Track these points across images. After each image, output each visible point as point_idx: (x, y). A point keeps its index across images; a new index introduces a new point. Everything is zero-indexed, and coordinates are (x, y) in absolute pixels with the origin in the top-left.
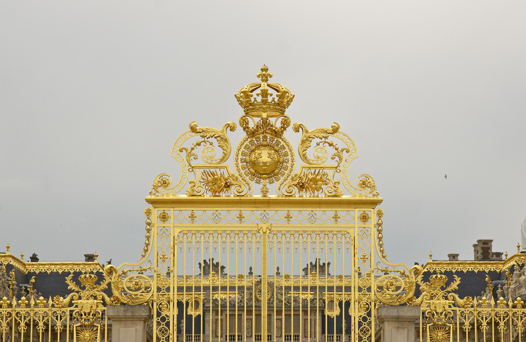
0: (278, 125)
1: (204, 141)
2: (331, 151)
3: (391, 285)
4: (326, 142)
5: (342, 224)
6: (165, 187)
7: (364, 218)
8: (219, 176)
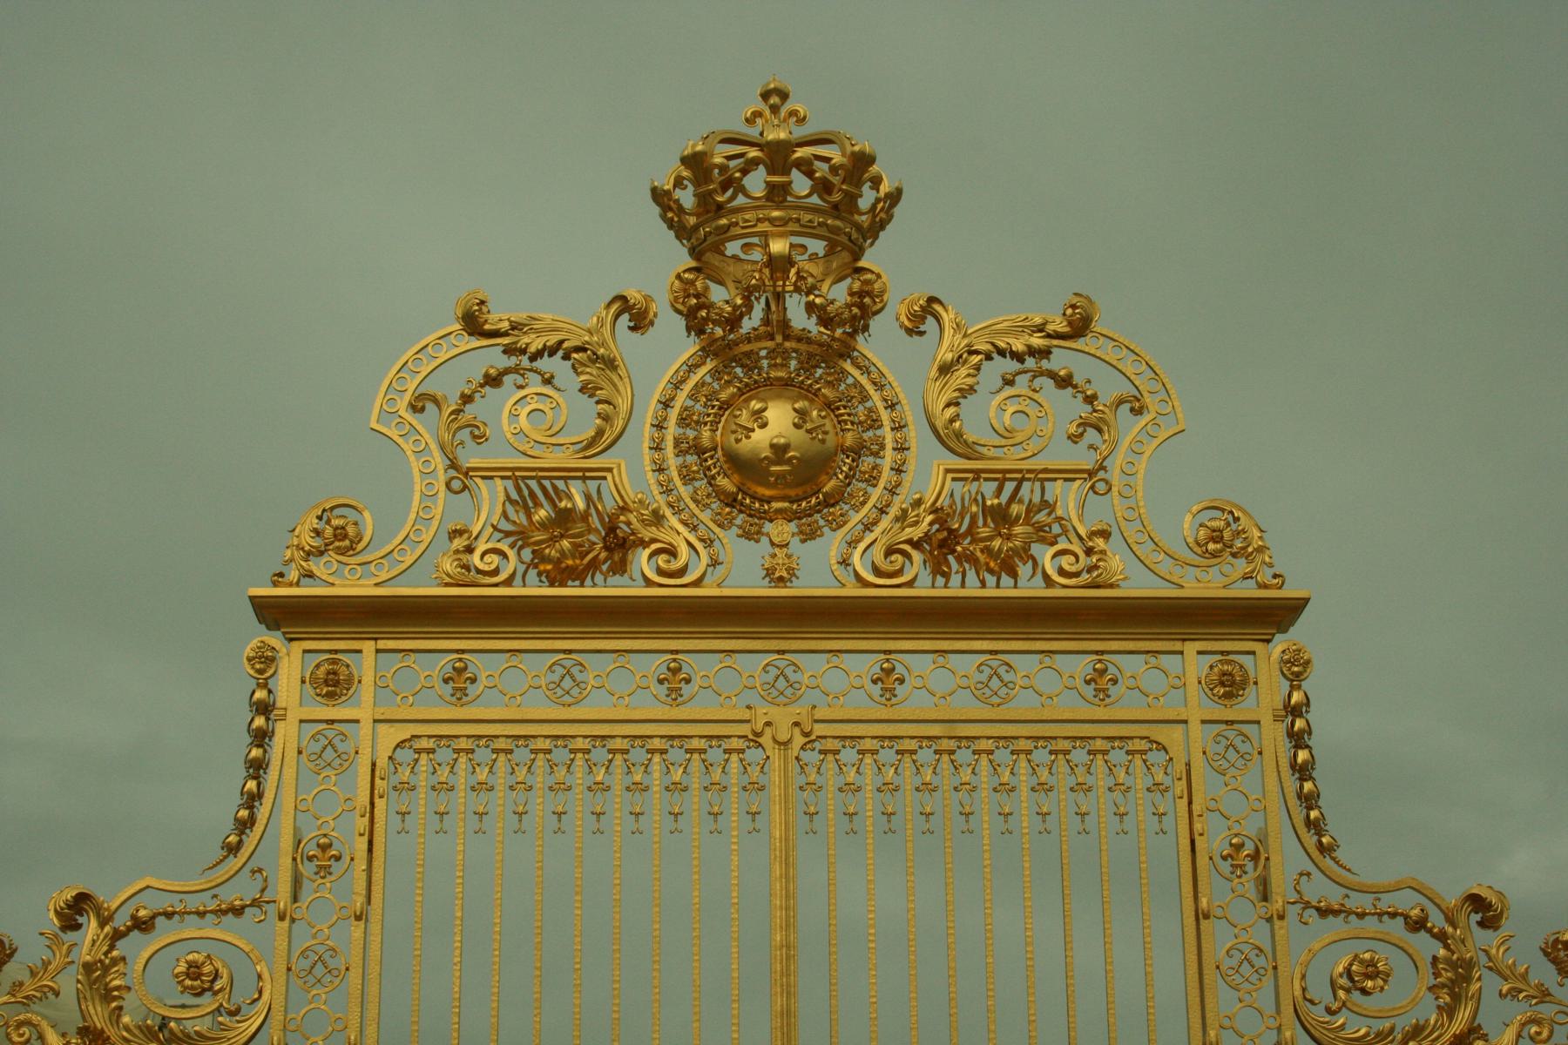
1: (515, 370)
2: (1067, 407)
3: (1368, 976)
5: (1125, 704)
6: (342, 552)
7: (1230, 685)
8: (581, 504)
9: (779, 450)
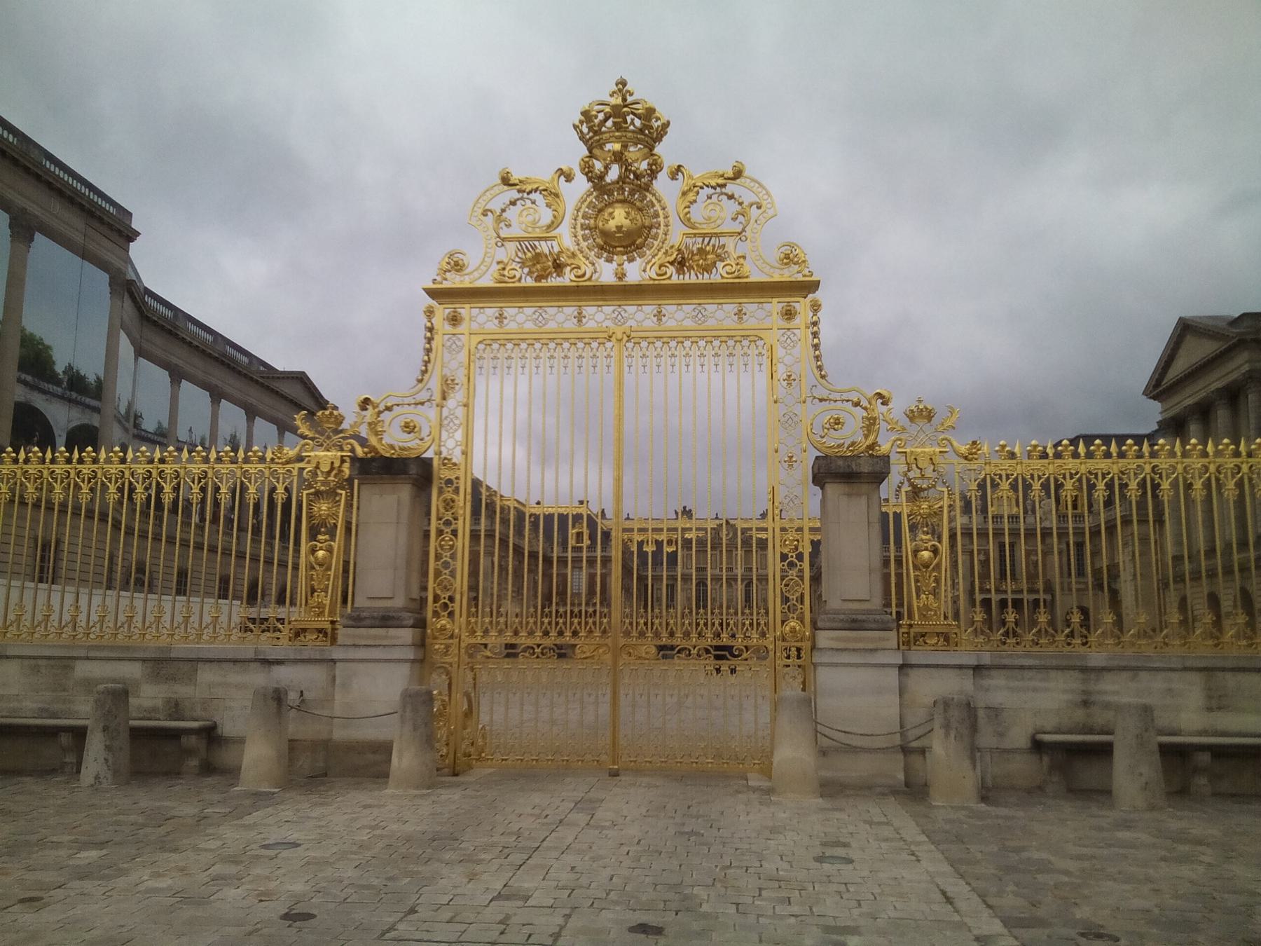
0: (644, 166)
1: (522, 198)
2: (733, 207)
4: (722, 193)
5: (750, 322)
7: (789, 314)
9: (619, 228)
